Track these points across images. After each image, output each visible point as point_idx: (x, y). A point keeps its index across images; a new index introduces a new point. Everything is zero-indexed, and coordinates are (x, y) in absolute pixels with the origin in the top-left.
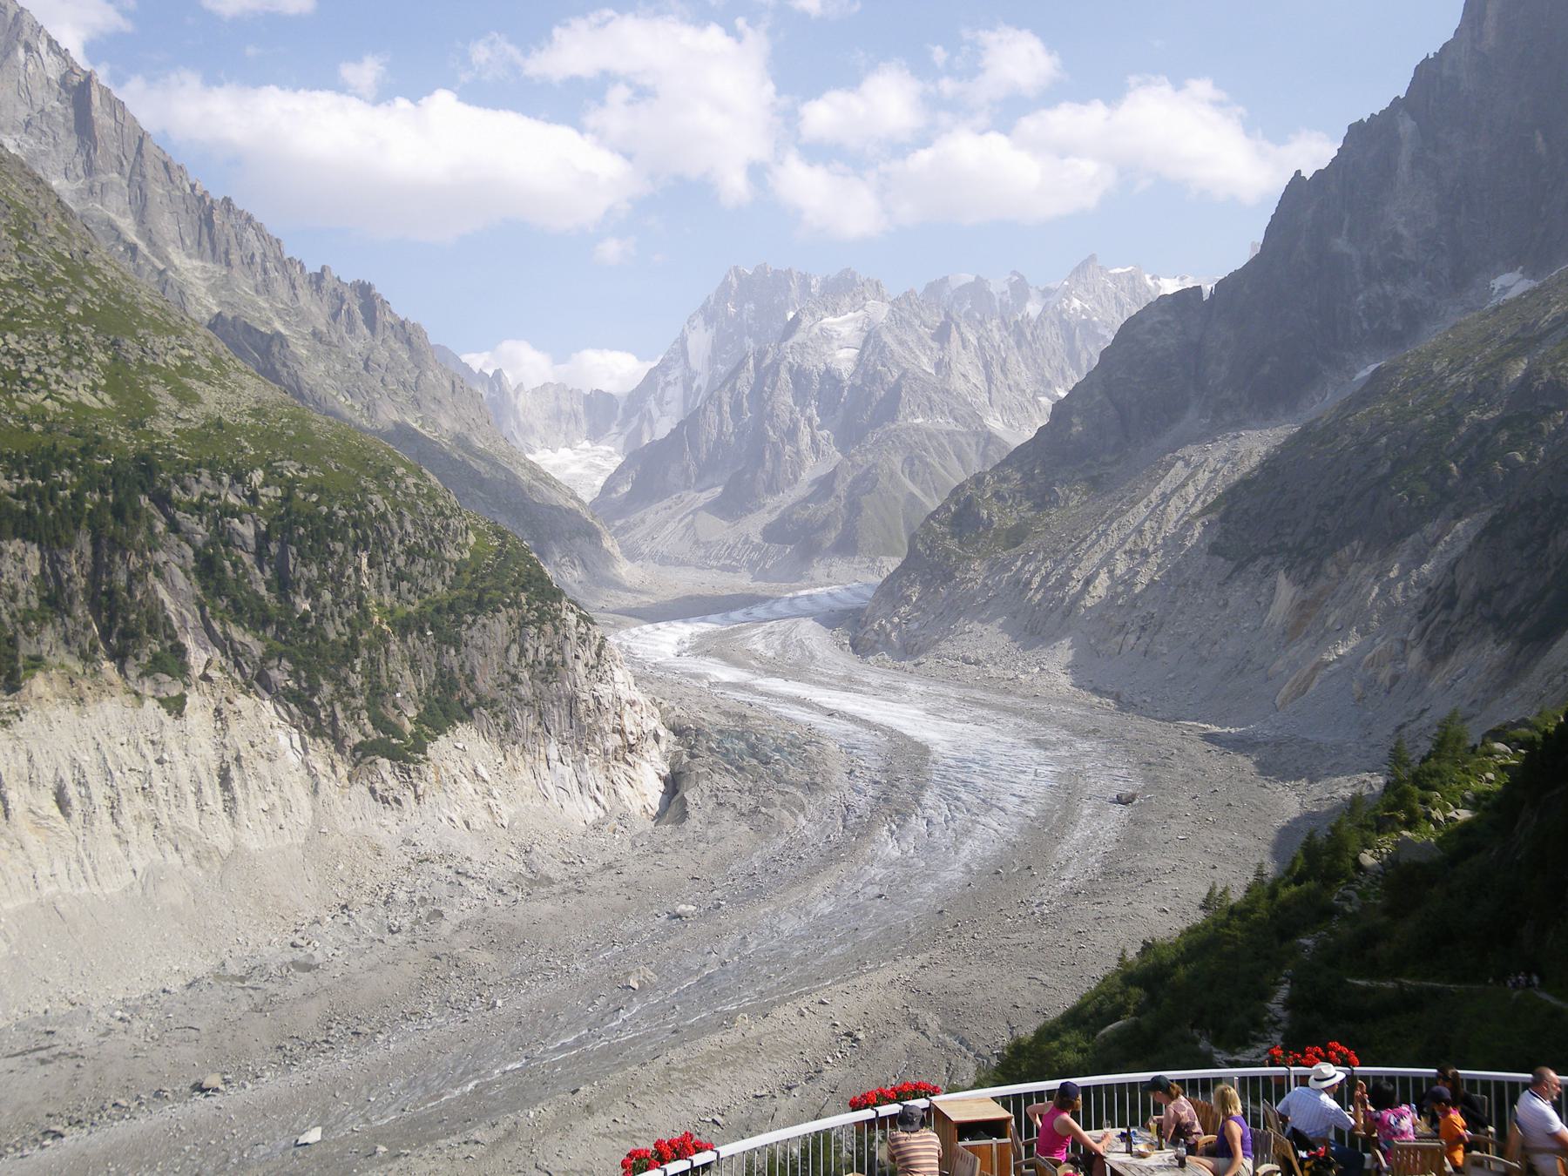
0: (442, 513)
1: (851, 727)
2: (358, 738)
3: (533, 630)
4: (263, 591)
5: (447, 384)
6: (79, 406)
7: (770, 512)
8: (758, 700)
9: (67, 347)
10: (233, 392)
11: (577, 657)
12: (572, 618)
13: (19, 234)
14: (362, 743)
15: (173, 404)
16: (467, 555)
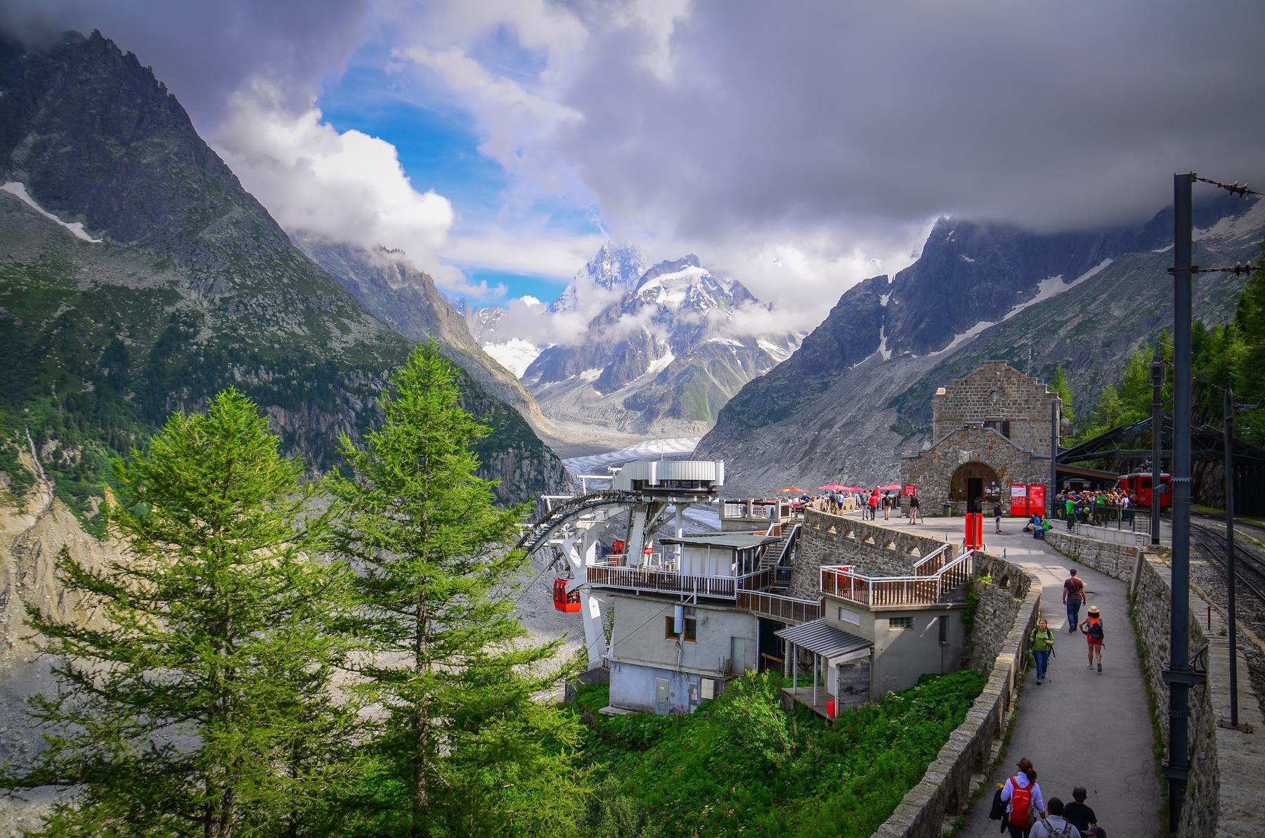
0: (477, 396)
3: (526, 462)
5: (445, 311)
6: (293, 334)
9: (285, 301)
12: (548, 456)
13: (256, 239)
15: (337, 332)
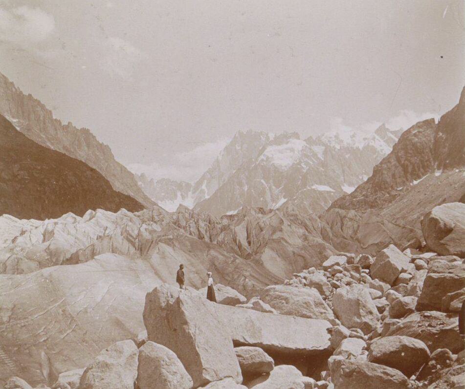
5: (119, 169)
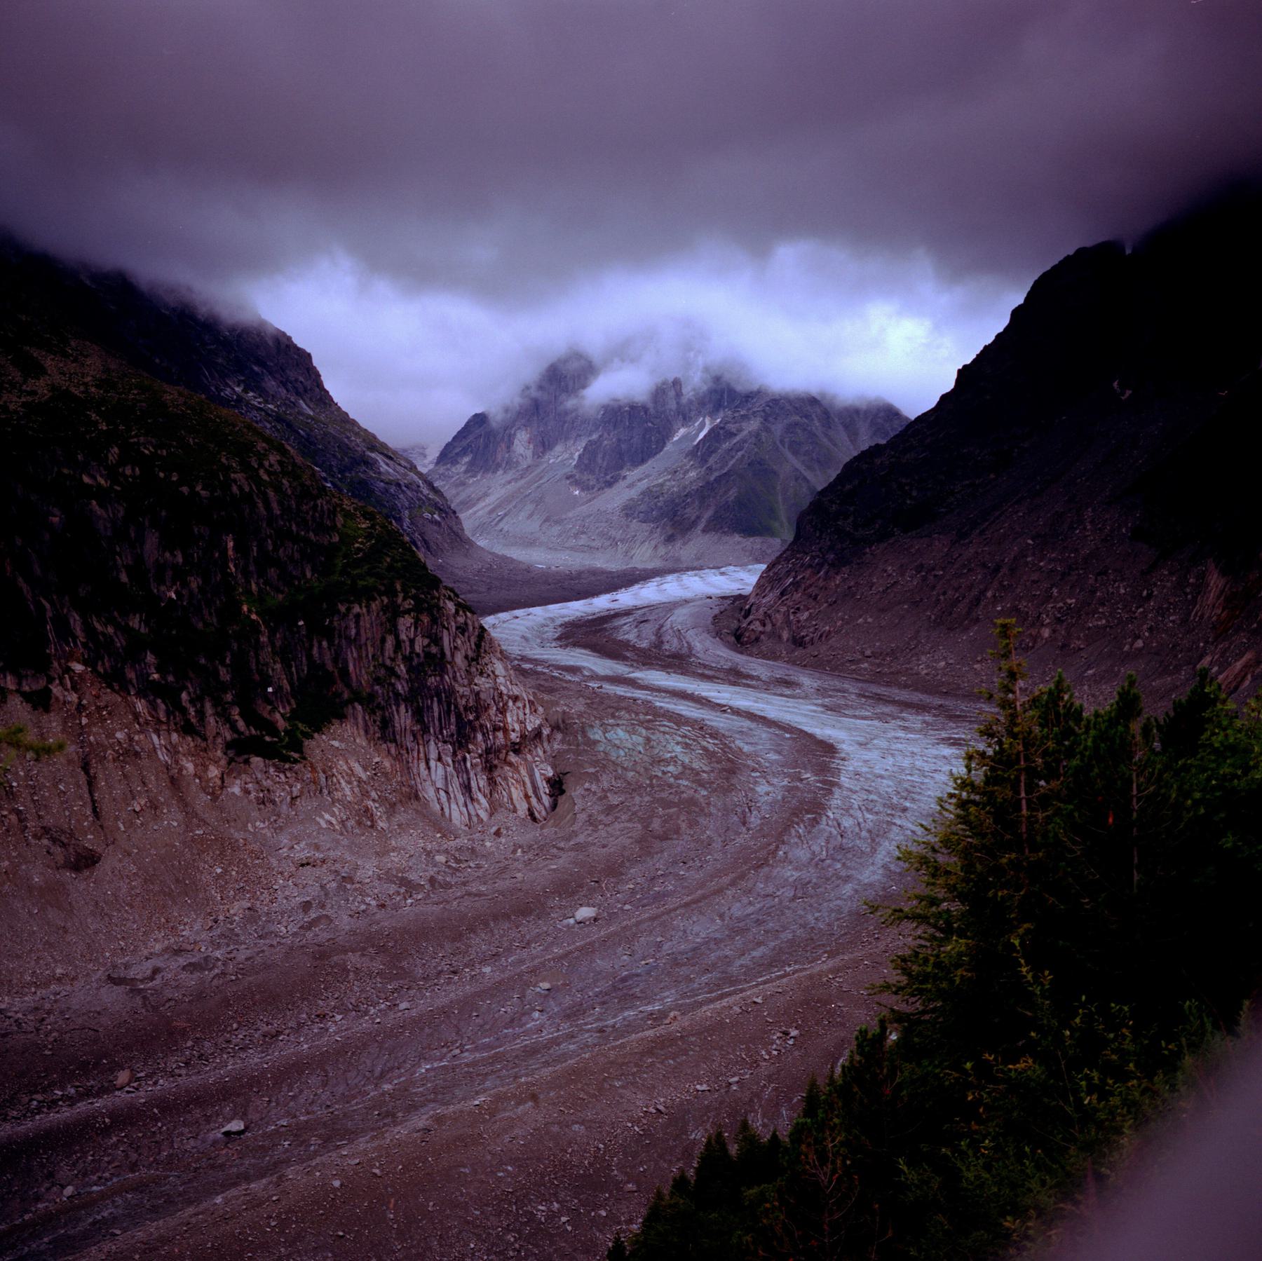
1: (747, 723)
2: (228, 735)
4: (124, 578)
7: (631, 486)
8: (639, 694)
10: (75, 361)
11: (456, 648)
12: (451, 606)
14: (233, 740)
15: (17, 375)
16: (336, 539)
